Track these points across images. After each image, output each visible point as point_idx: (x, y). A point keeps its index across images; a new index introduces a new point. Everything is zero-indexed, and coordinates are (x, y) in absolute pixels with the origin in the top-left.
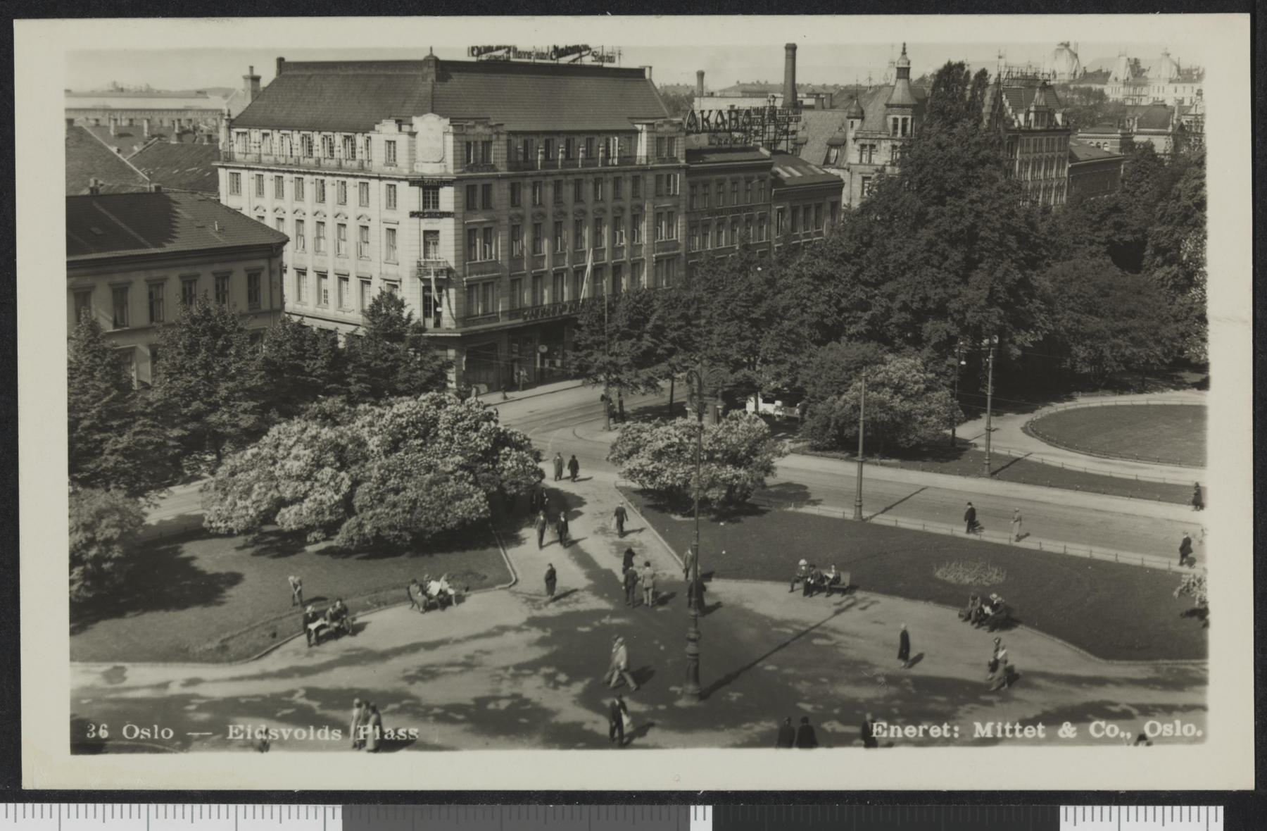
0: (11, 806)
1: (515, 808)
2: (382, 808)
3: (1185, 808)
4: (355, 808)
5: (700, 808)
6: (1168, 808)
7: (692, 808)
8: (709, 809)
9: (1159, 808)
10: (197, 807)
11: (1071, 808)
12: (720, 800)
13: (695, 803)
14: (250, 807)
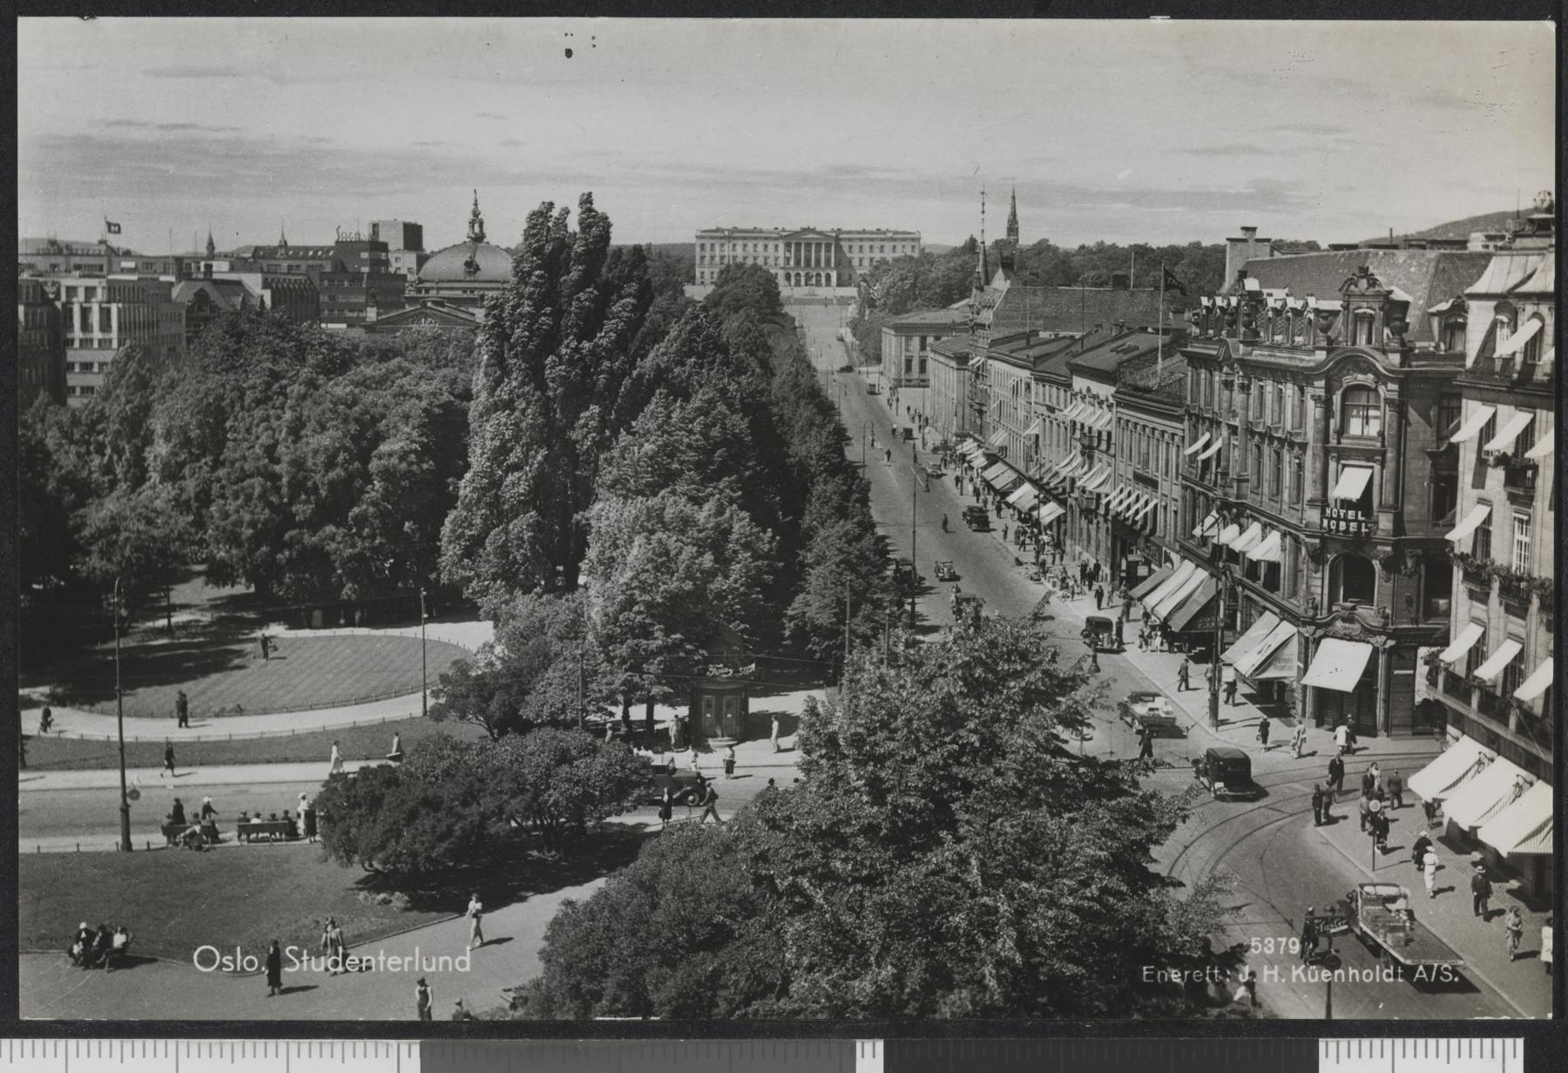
3: (1476, 1041)
5: (868, 1044)
6: (1454, 1041)
9: (1443, 1042)
11: (1332, 1042)
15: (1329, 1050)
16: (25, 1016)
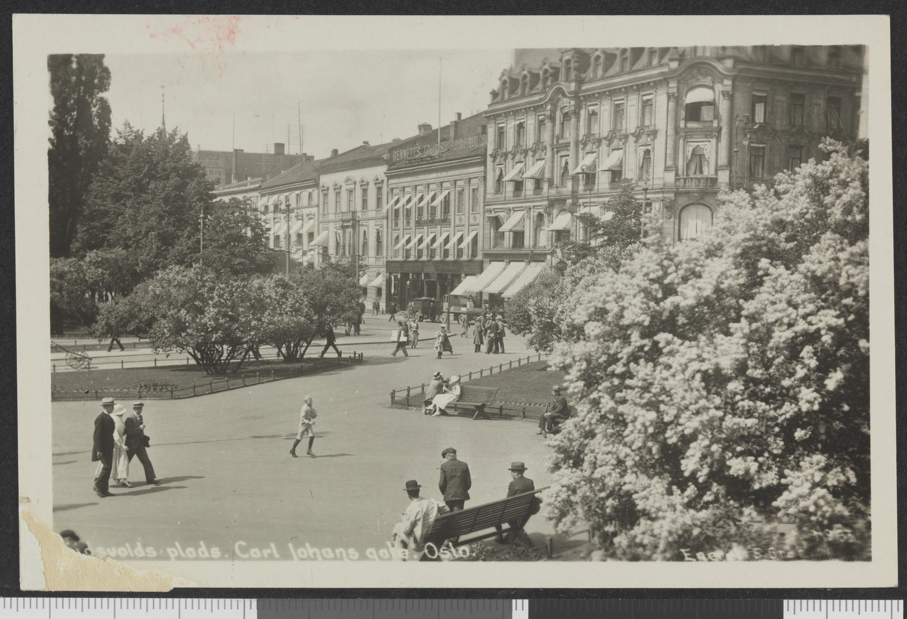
0: (8, 599)
1: (384, 601)
2: (287, 601)
4: (267, 601)
5: (520, 601)
8: (526, 602)
11: (791, 602)
13: (516, 598)
14: (189, 600)
15: (789, 605)
16: (24, 587)
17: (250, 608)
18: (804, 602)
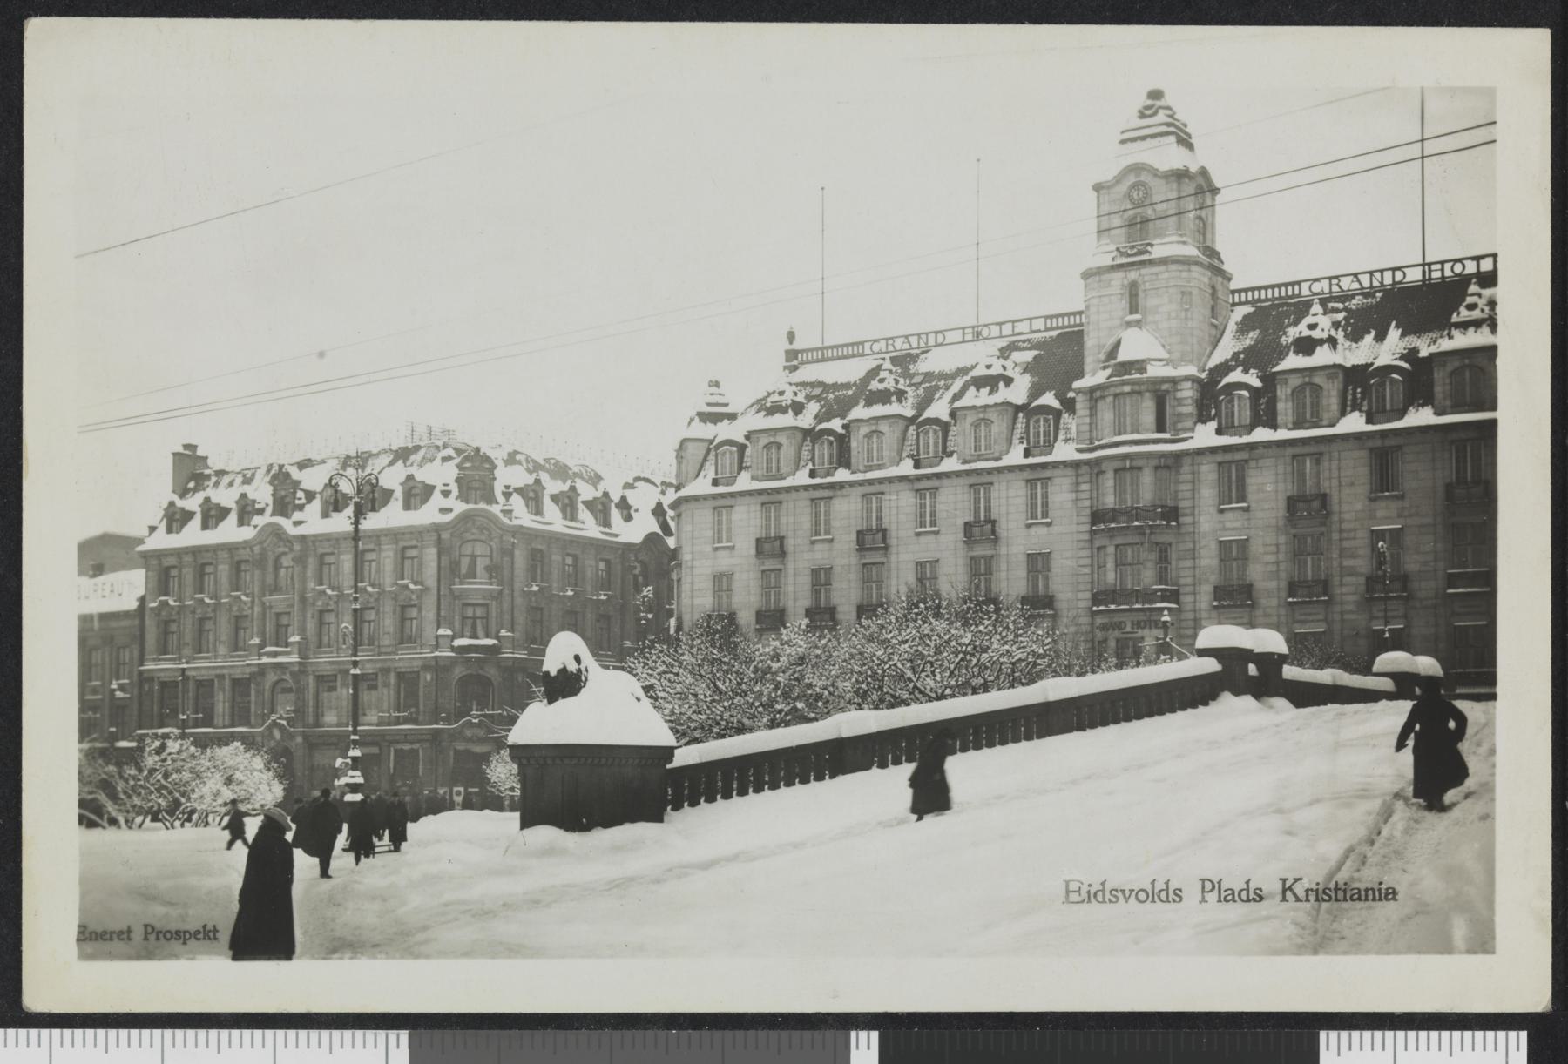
4: (425, 1034)
5: (863, 1034)
7: (853, 1034)
8: (875, 1035)
10: (224, 1033)
11: (1333, 1034)
12: (888, 1024)
15: (1328, 1040)
17: (397, 1048)
18: (1356, 1034)
